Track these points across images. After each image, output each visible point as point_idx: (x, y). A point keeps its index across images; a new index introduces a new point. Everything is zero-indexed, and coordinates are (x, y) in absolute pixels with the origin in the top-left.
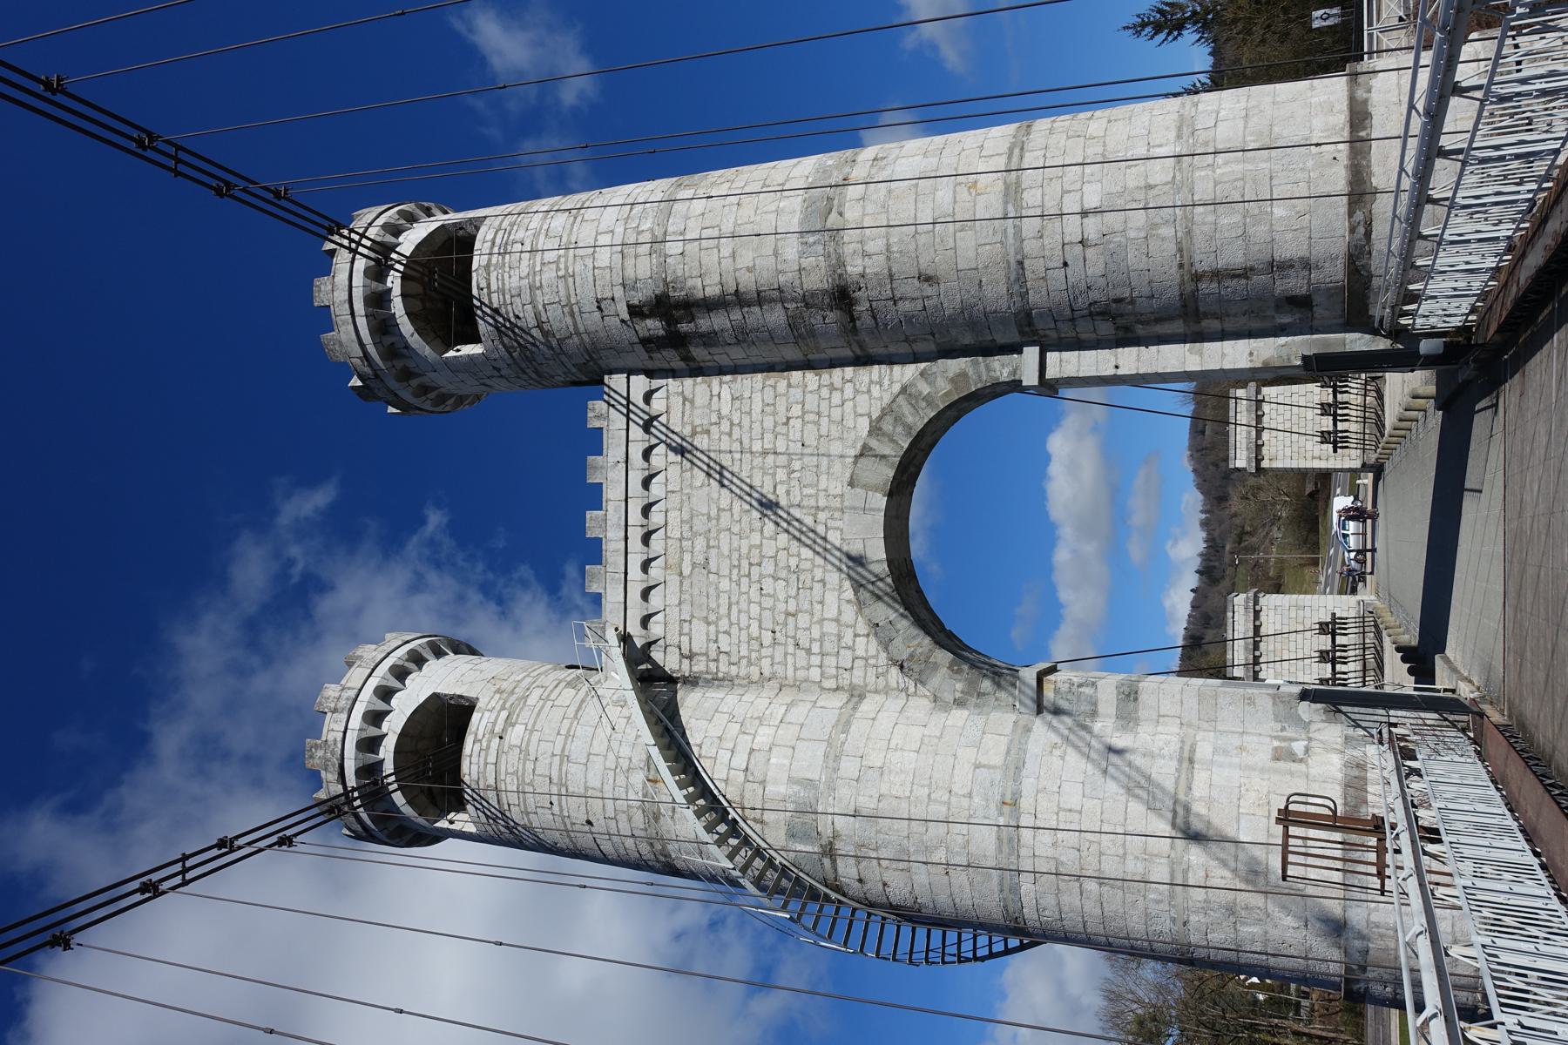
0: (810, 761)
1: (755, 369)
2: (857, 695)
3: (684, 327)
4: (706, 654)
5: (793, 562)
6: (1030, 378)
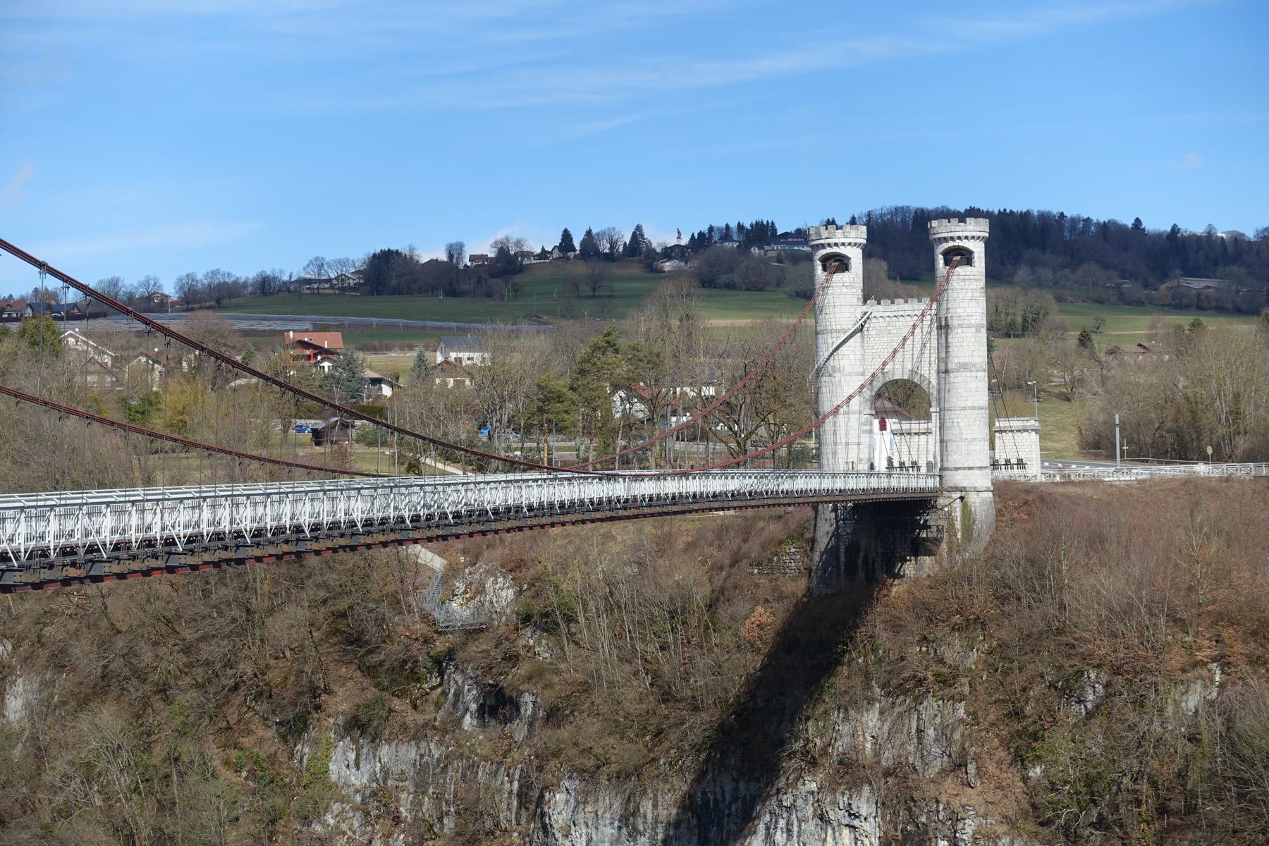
0: (848, 369)
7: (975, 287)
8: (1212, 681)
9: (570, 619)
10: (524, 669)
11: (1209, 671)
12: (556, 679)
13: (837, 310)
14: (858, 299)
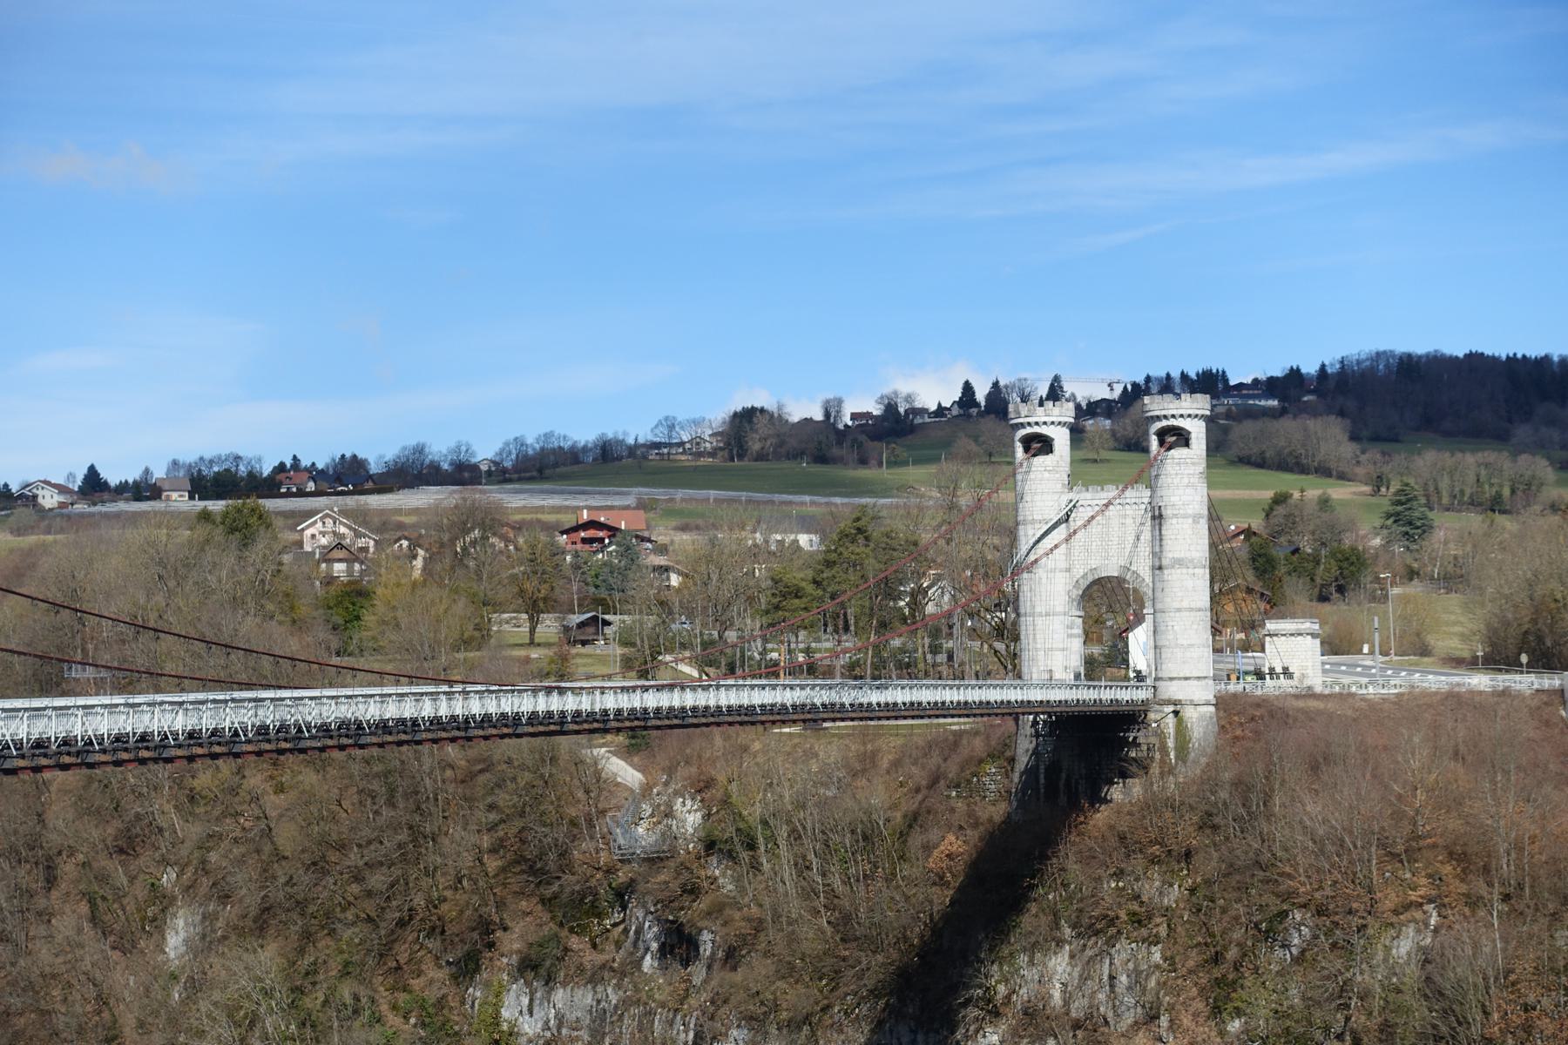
2: (1068, 570)
7: (1192, 472)
8: (1427, 925)
9: (751, 846)
10: (703, 904)
11: (1425, 913)
12: (737, 915)
13: (1037, 498)
14: (1063, 485)
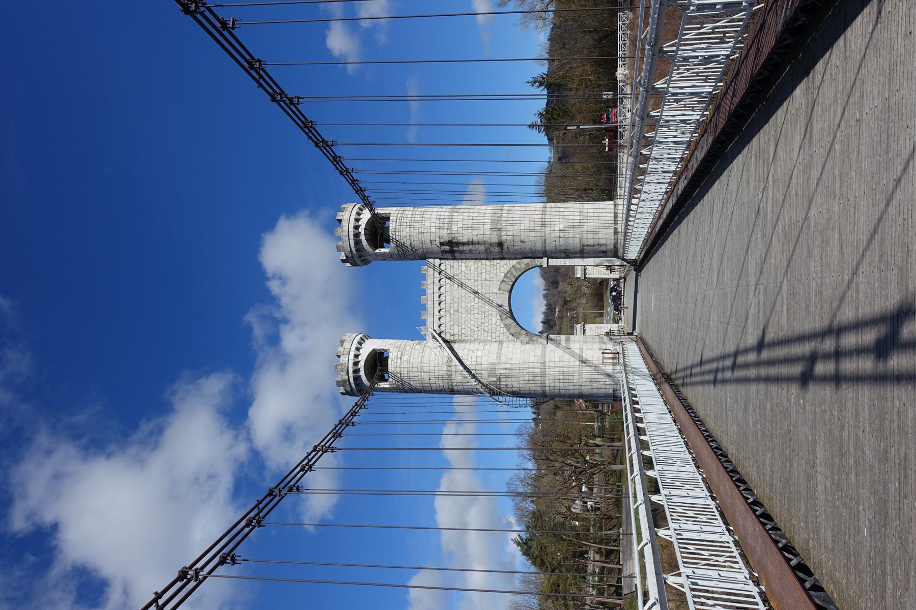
0: (493, 358)
1: (472, 259)
2: (501, 342)
3: (455, 249)
4: (458, 334)
5: (483, 310)
6: (545, 265)
